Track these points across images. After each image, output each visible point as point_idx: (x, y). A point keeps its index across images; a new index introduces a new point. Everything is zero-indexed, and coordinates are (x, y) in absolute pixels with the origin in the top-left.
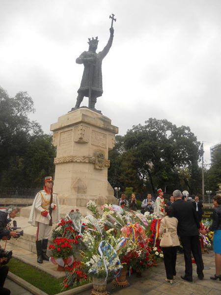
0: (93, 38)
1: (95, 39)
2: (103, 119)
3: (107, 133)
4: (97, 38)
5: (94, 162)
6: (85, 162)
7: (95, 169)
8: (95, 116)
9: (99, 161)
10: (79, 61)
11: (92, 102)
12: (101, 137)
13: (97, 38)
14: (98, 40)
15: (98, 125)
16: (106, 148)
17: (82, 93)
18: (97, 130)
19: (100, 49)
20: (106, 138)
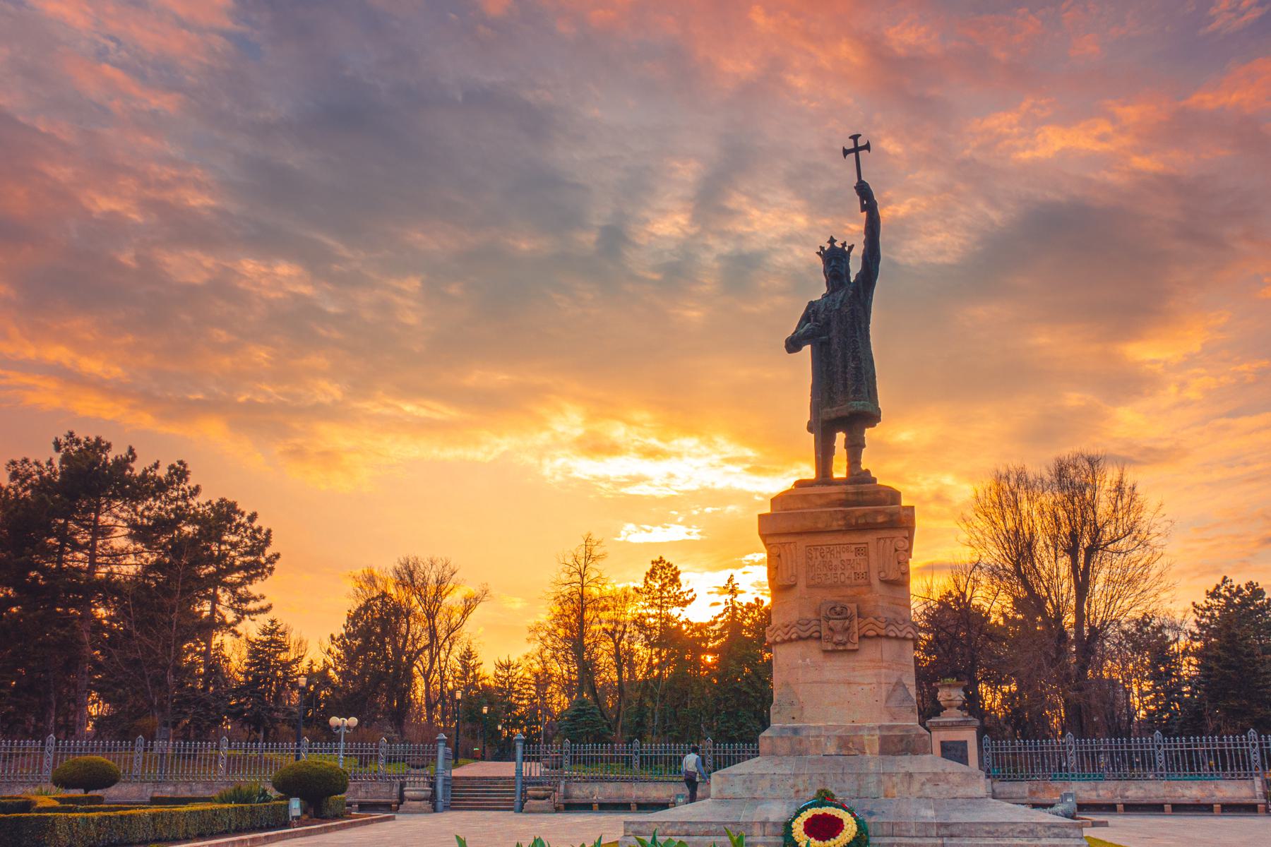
0: (822, 248)
1: (827, 247)
2: (851, 497)
3: (870, 538)
4: (832, 241)
5: (816, 635)
6: (790, 640)
7: (825, 651)
8: (819, 502)
9: (831, 629)
10: (793, 345)
11: (855, 448)
12: (845, 556)
13: (832, 241)
14: (838, 245)
15: (821, 525)
16: (870, 584)
17: (823, 429)
18: (828, 540)
19: (855, 267)
20: (867, 554)
